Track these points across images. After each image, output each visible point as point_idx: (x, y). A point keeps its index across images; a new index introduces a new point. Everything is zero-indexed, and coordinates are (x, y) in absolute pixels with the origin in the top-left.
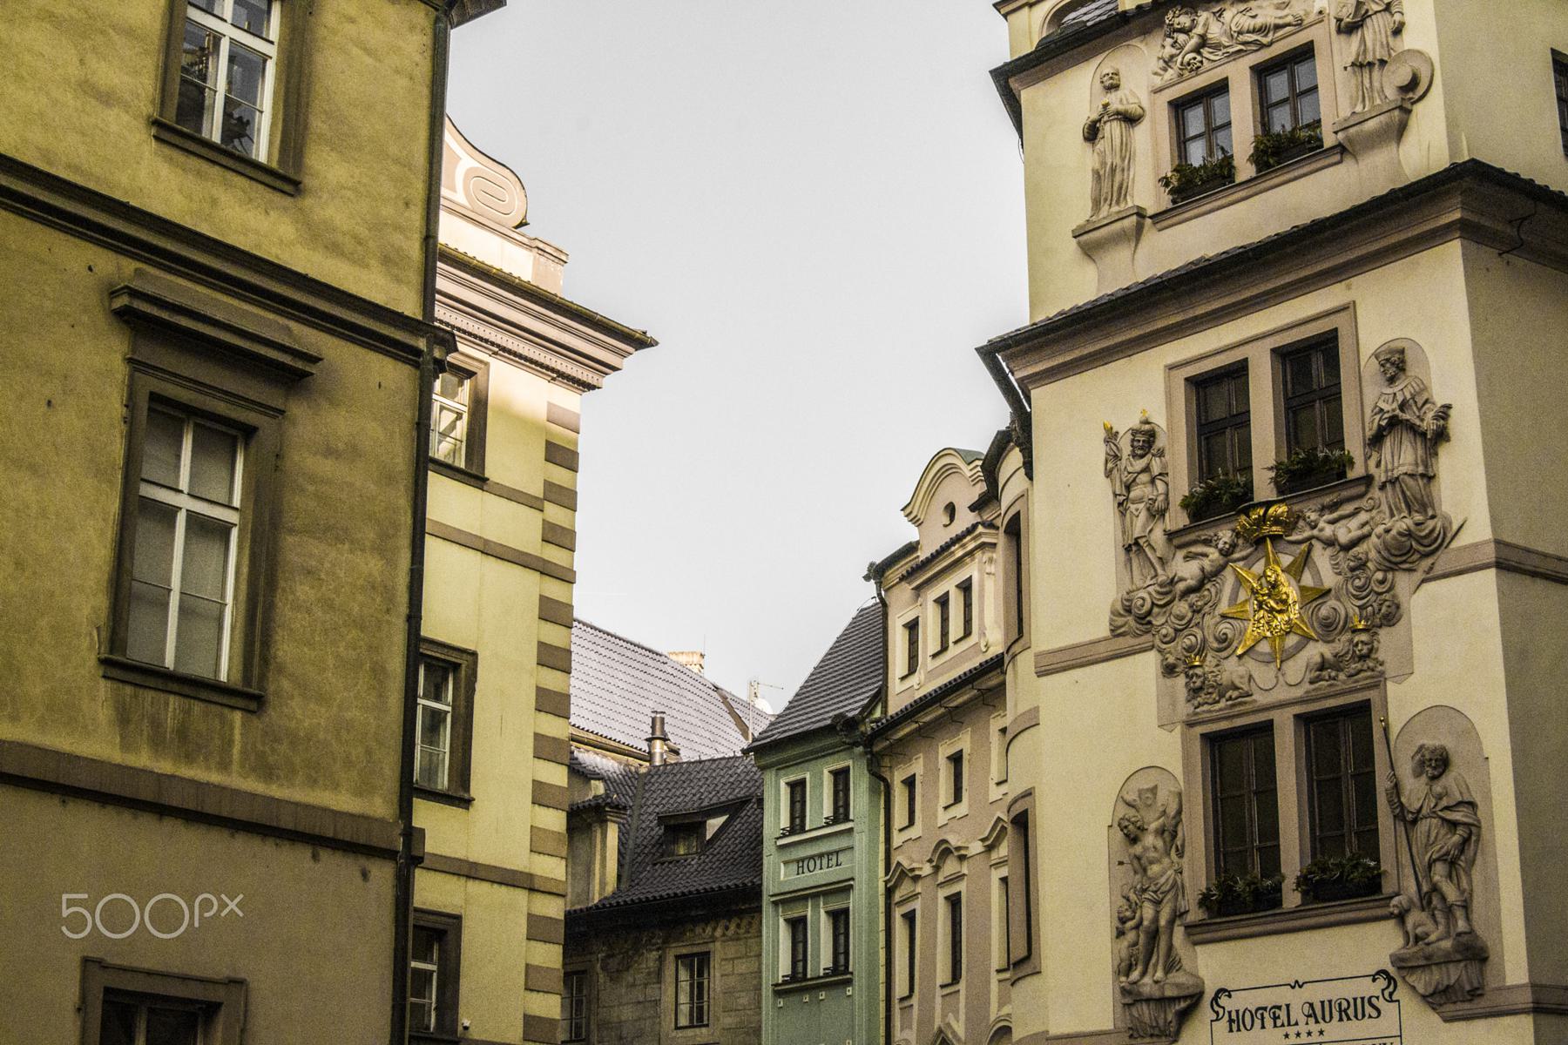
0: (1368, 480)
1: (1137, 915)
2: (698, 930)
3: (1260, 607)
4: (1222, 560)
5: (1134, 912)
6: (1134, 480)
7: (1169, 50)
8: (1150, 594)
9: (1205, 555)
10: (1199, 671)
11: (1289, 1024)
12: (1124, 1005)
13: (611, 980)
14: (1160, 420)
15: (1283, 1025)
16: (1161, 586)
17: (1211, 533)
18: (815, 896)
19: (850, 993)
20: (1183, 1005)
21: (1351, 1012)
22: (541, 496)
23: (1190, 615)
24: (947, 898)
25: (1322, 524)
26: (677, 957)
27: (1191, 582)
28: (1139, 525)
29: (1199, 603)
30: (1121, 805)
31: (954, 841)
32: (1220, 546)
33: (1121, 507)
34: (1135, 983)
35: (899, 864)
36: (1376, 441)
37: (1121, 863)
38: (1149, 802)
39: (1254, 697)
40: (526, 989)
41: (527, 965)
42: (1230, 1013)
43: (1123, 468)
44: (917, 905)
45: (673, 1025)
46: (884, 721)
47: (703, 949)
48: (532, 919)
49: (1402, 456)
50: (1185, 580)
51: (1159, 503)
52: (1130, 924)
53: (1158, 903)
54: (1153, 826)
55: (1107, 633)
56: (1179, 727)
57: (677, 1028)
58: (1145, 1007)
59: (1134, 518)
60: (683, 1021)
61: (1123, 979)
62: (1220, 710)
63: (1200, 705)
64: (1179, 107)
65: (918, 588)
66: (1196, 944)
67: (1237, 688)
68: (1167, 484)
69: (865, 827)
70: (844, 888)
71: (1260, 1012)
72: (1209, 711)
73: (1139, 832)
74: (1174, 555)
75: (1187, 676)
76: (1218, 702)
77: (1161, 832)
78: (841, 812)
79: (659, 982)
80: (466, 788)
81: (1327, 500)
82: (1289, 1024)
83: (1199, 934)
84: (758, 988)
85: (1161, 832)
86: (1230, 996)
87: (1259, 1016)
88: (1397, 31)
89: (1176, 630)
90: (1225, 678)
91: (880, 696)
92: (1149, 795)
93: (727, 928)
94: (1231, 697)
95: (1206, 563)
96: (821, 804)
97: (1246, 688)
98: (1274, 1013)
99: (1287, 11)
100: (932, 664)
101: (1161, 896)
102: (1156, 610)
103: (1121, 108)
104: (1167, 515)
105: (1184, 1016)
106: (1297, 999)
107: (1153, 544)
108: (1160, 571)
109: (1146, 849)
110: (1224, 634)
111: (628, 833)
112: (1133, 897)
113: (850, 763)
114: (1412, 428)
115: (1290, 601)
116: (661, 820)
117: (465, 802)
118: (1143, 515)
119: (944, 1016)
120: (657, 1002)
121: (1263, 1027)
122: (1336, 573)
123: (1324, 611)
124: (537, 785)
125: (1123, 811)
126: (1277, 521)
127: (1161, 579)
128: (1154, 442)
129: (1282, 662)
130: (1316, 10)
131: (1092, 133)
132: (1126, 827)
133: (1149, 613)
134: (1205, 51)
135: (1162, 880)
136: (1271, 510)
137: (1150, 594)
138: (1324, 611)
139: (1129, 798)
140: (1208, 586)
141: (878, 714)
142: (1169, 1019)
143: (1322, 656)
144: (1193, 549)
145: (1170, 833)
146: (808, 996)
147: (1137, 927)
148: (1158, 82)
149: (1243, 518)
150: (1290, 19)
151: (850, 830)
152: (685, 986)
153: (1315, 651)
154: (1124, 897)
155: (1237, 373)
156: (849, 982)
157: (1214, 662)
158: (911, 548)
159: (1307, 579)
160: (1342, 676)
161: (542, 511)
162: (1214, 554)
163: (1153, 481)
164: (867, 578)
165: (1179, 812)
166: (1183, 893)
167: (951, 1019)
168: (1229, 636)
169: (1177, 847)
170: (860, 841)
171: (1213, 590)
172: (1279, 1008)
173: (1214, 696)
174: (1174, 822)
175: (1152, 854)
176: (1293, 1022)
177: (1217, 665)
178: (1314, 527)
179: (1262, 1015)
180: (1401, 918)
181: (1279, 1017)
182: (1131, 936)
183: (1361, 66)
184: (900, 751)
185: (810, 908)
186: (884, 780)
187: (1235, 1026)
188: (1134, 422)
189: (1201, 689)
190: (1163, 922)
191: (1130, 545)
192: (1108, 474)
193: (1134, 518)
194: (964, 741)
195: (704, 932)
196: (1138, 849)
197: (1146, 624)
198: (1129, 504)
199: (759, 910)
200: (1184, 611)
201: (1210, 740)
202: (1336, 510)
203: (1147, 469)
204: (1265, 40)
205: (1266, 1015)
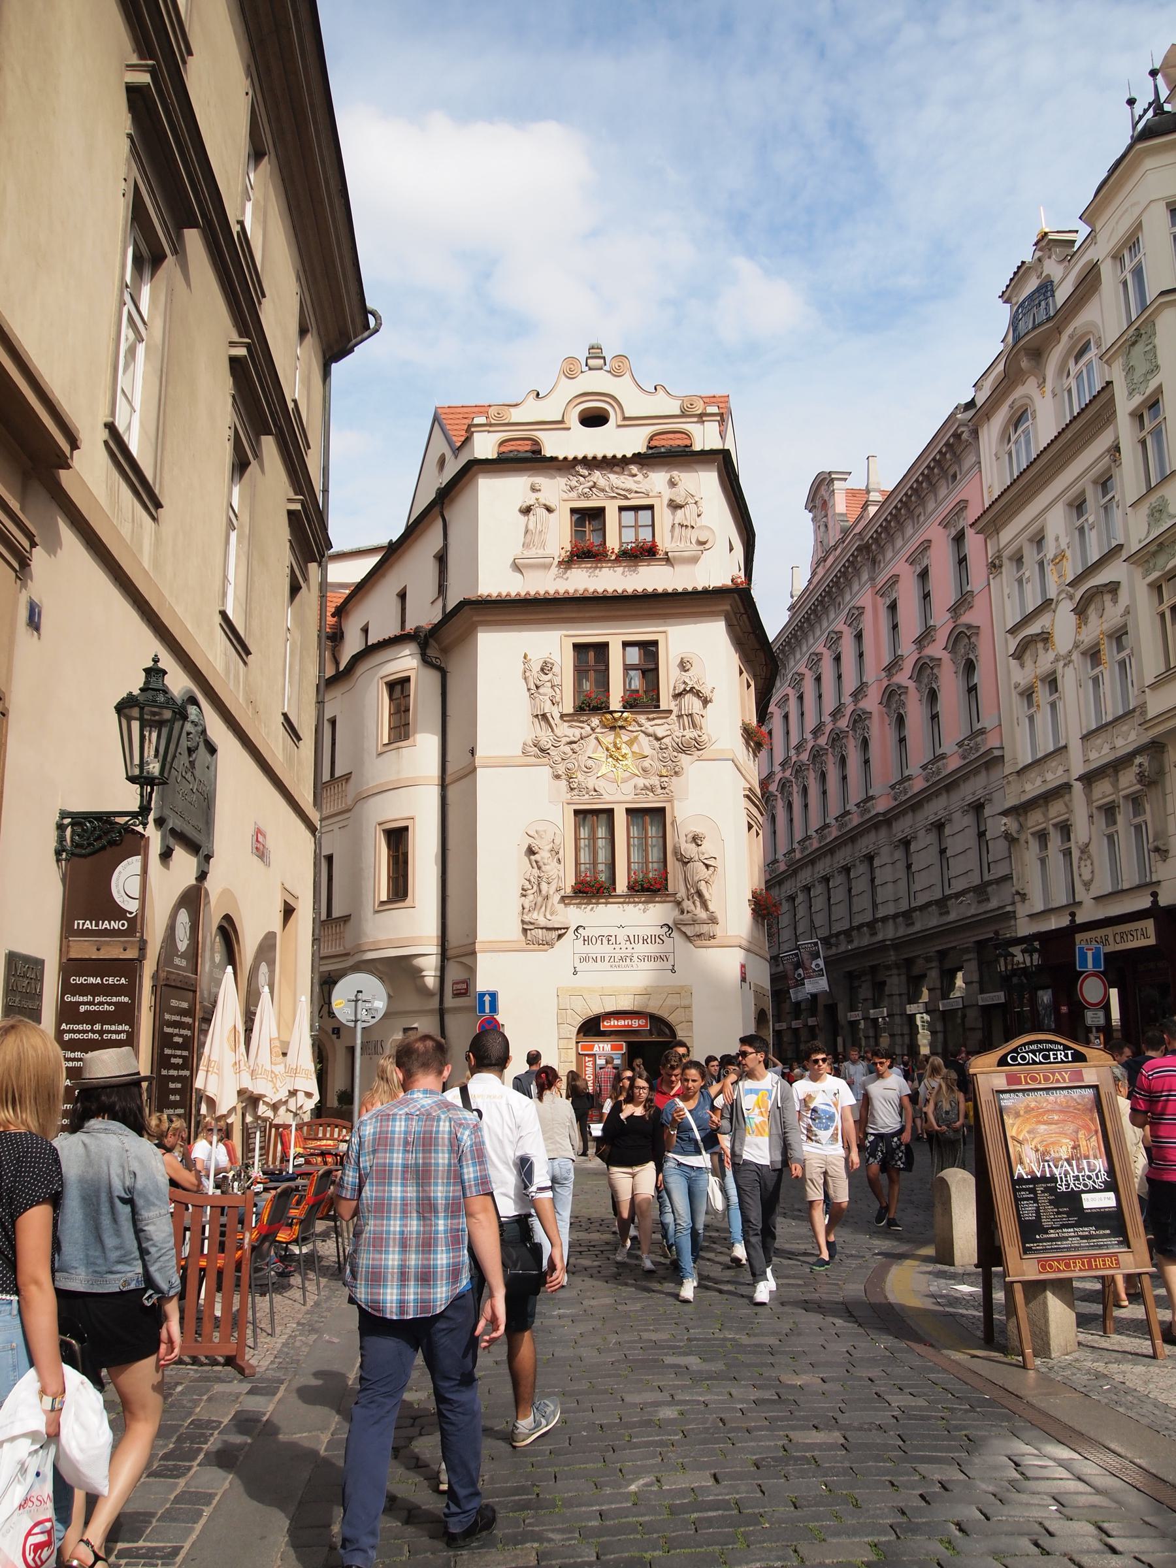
0: (670, 712)
3: (611, 756)
7: (574, 483)
9: (582, 728)
14: (556, 658)
17: (585, 718)
20: (563, 931)
21: (649, 941)
27: (573, 739)
28: (548, 708)
36: (678, 696)
49: (692, 703)
51: (558, 699)
52: (529, 892)
64: (573, 511)
67: (595, 791)
81: (651, 716)
88: (699, 516)
90: (591, 787)
95: (582, 731)
99: (640, 486)
103: (548, 503)
105: (560, 936)
106: (621, 935)
109: (542, 858)
114: (698, 694)
126: (626, 720)
130: (657, 489)
131: (526, 511)
134: (593, 489)
135: (551, 874)
136: (625, 715)
138: (646, 763)
148: (565, 496)
149: (609, 716)
150: (643, 490)
153: (641, 782)
155: (602, 649)
159: (635, 748)
160: (651, 794)
162: (588, 728)
175: (546, 861)
180: (679, 903)
182: (531, 897)
183: (682, 526)
190: (551, 893)
196: (537, 857)
204: (629, 496)
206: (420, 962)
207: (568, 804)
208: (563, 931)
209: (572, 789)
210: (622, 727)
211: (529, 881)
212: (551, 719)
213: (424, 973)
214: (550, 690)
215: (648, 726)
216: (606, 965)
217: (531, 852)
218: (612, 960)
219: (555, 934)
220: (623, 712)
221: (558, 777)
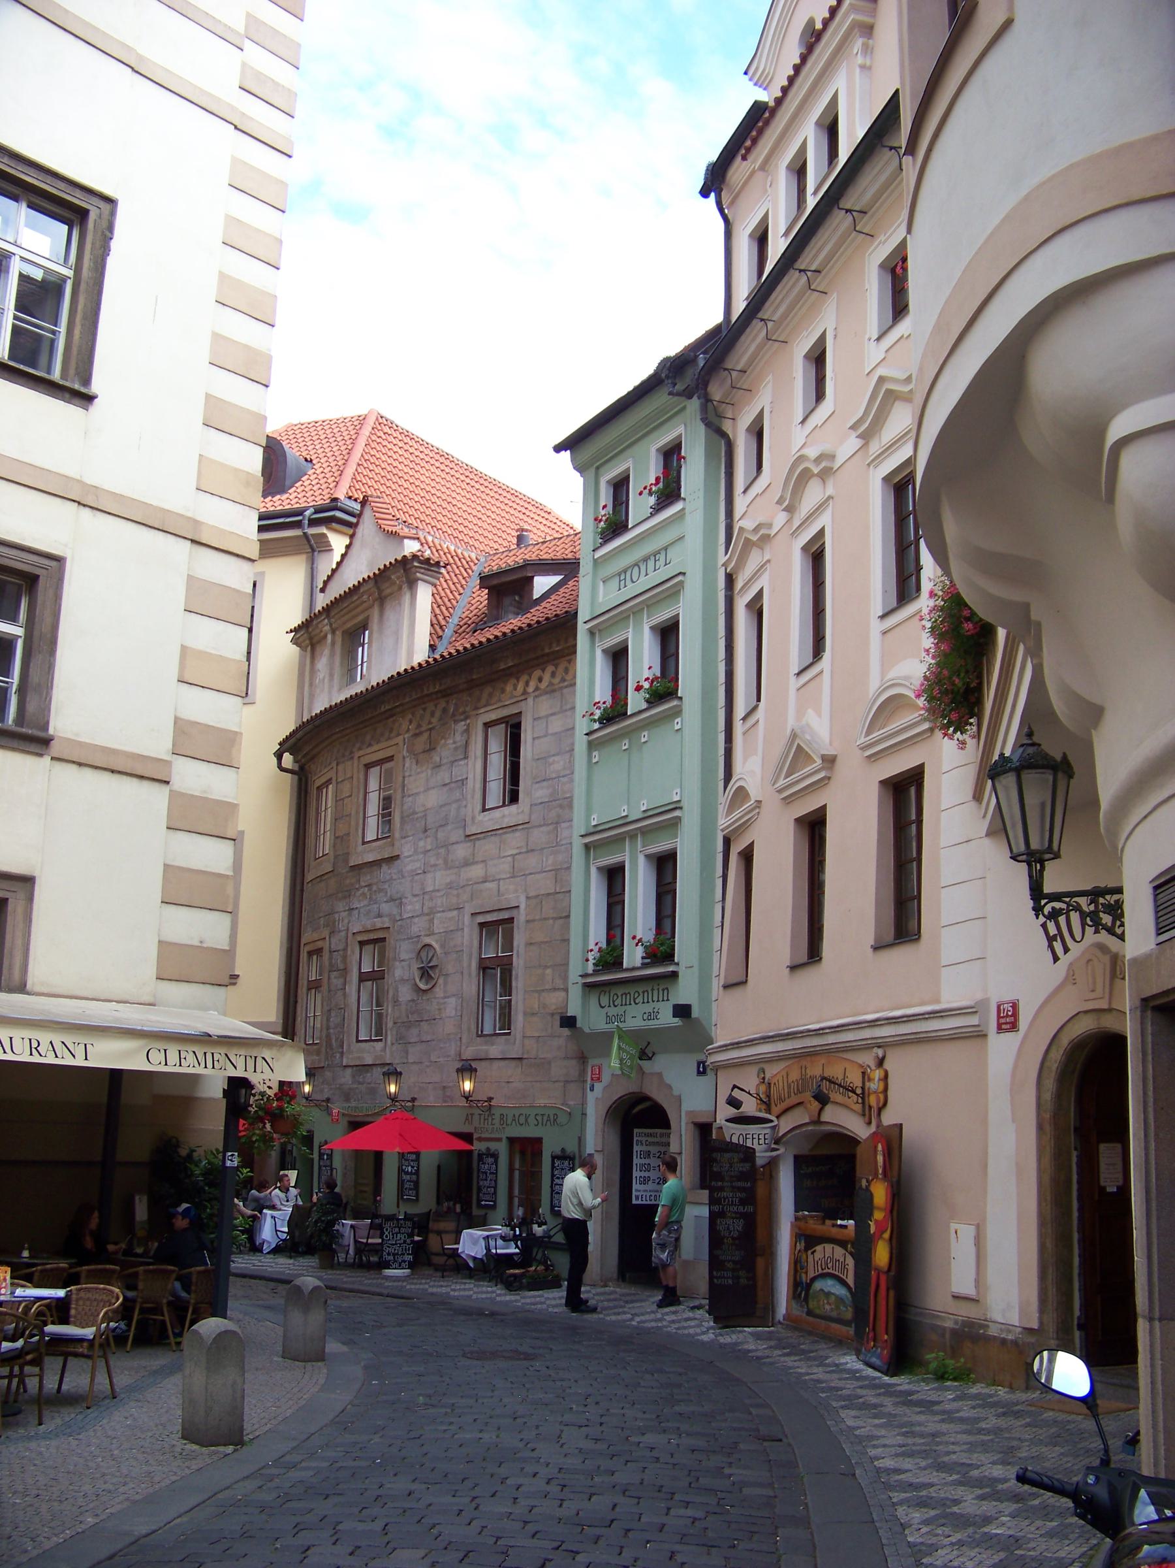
2: (509, 688)
13: (417, 762)
18: (636, 612)
26: (487, 725)
35: (741, 529)
41: (184, 649)
45: (479, 807)
47: (514, 710)
48: (193, 583)
57: (484, 810)
60: (494, 799)
69: (700, 503)
70: (671, 589)
79: (466, 758)
80: (87, 380)
93: (540, 680)
111: (454, 608)
113: (680, 430)
116: (486, 580)
117: (86, 399)
119: (800, 712)
120: (463, 782)
146: (627, 741)
151: (681, 514)
156: (677, 712)
164: (704, 193)
167: (811, 717)
184: (743, 390)
186: (723, 434)
195: (515, 689)
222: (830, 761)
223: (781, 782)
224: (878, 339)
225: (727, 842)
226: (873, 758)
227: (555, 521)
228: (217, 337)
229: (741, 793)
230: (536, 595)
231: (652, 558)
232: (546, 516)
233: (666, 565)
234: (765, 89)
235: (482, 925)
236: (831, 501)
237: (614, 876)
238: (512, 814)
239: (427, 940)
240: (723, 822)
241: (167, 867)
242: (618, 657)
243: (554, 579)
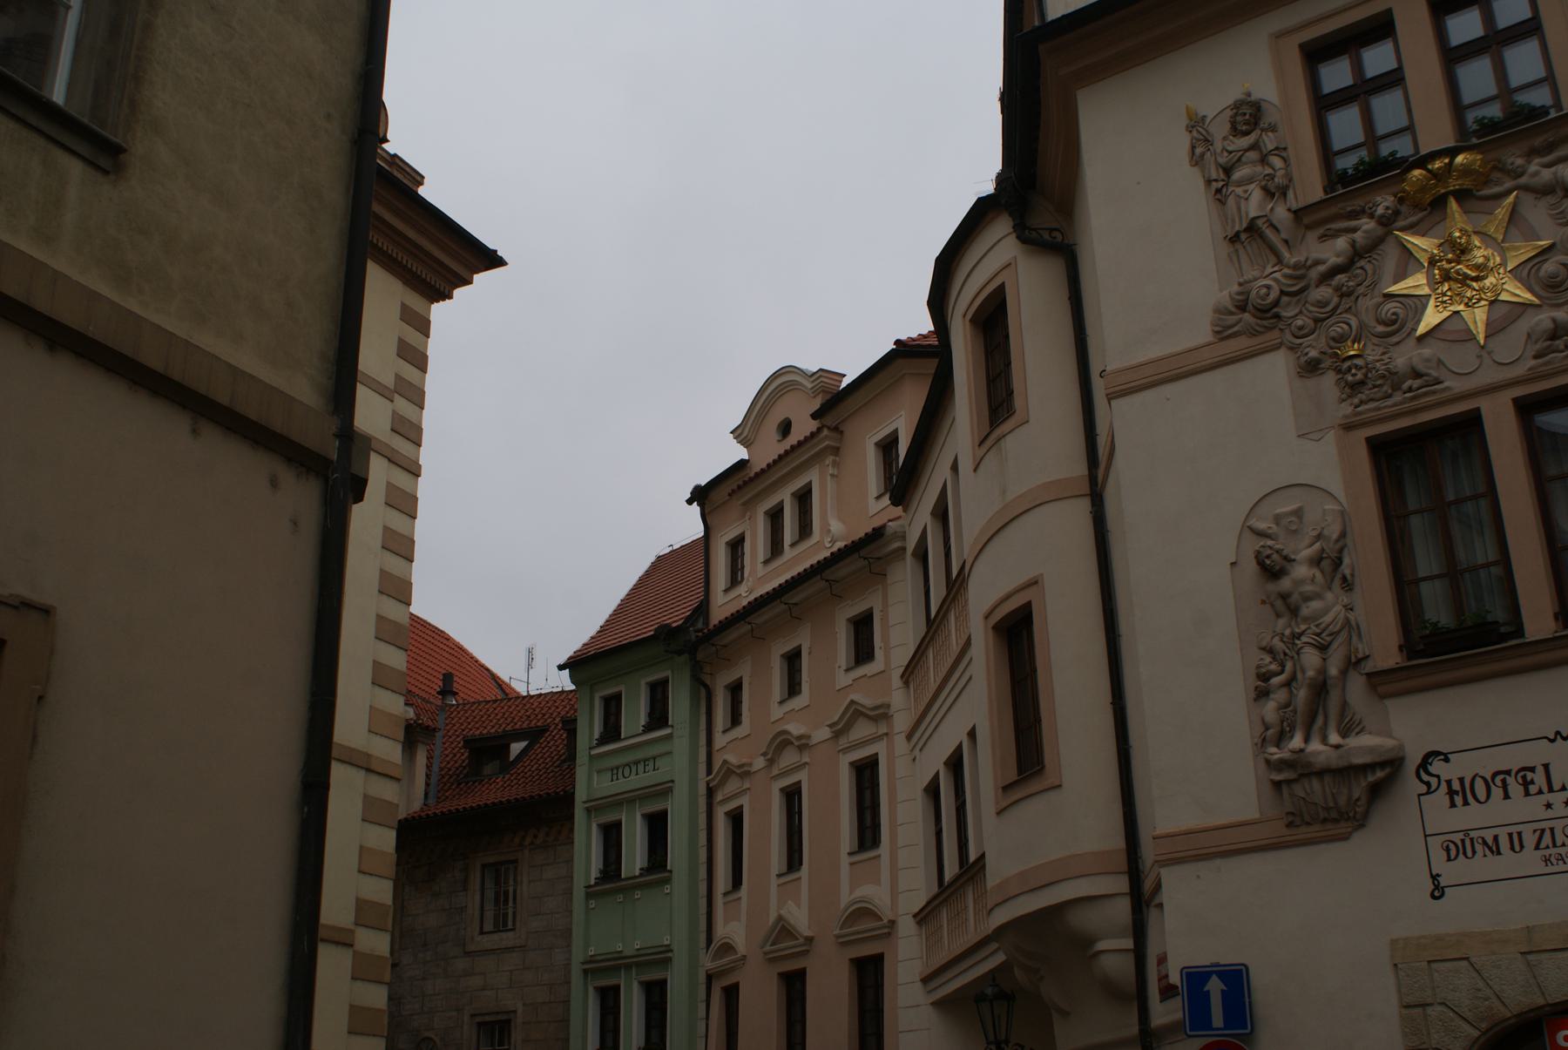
1: (1289, 666)
3: (1446, 277)
4: (1380, 231)
5: (1283, 666)
6: (1239, 159)
8: (1276, 280)
9: (1355, 230)
10: (1358, 362)
11: (1551, 790)
12: (1277, 785)
14: (1265, 88)
15: (1540, 792)
16: (1296, 267)
17: (1357, 203)
18: (631, 801)
19: (668, 891)
20: (1380, 774)
22: (392, 388)
23: (1336, 300)
24: (782, 790)
25: (1533, 168)
27: (1334, 260)
28: (1255, 204)
29: (1351, 284)
30: (1248, 534)
31: (795, 729)
32: (1380, 211)
33: (1220, 196)
34: (1302, 751)
35: (725, 762)
37: (1263, 602)
38: (1294, 528)
39: (1446, 384)
40: (360, 871)
42: (1449, 782)
43: (1219, 150)
44: (744, 801)
46: (706, 631)
50: (1323, 262)
51: (1279, 179)
52: (1276, 680)
53: (1323, 648)
54: (1306, 553)
55: (1210, 338)
56: (1331, 436)
57: (482, 933)
58: (1316, 784)
59: (1243, 203)
60: (488, 927)
61: (1273, 750)
62: (1395, 405)
63: (1362, 402)
65: (744, 504)
66: (1383, 697)
67: (1417, 375)
68: (1283, 158)
70: (665, 790)
71: (1502, 776)
72: (1378, 409)
73: (1285, 563)
74: (1304, 236)
75: (1339, 371)
76: (1390, 396)
77: (1316, 561)
78: (658, 718)
79: (465, 889)
81: (1538, 141)
82: (1551, 790)
83: (1383, 683)
84: (569, 893)
85: (1316, 561)
86: (1447, 760)
87: (1499, 784)
89: (1317, 321)
91: (703, 609)
92: (1293, 519)
93: (535, 837)
94: (1410, 390)
95: (1358, 236)
96: (635, 714)
97: (1434, 373)
98: (1524, 777)
100: (761, 570)
101: (1328, 639)
102: (1285, 299)
104: (1290, 195)
105: (1377, 791)
107: (1275, 222)
108: (1286, 254)
109: (1299, 583)
110: (1394, 314)
112: (1277, 644)
113: (668, 673)
115: (1491, 264)
116: (469, 743)
118: (1257, 195)
121: (1507, 796)
122: (1560, 224)
123: (1550, 267)
124: (377, 665)
125: (1255, 544)
126: (1466, 171)
127: (1293, 260)
128: (1260, 119)
129: (1486, 337)
132: (1268, 557)
133: (1276, 303)
135: (1327, 619)
136: (1460, 159)
137: (1276, 280)
138: (1550, 267)
139: (1261, 526)
140: (1358, 265)
141: (700, 625)
142: (1356, 794)
143: (1554, 320)
144: (1334, 226)
145: (1331, 562)
146: (621, 896)
147: (1288, 684)
149: (1417, 172)
151: (669, 737)
152: (490, 894)
153: (1544, 319)
154: (1263, 649)
156: (668, 881)
157: (1381, 350)
158: (741, 465)
161: (392, 401)
163: (1263, 160)
164: (690, 502)
165: (1343, 535)
166: (1360, 635)
168: (1401, 316)
169: (1344, 579)
170: (681, 745)
171: (1369, 267)
172: (1532, 769)
173: (1385, 388)
174: (1338, 546)
175: (1308, 588)
176: (1556, 786)
177: (1384, 354)
178: (1521, 175)
179: (1504, 781)
181: (1532, 782)
185: (624, 814)
187: (1458, 800)
188: (1234, 94)
189: (1362, 383)
190: (1333, 671)
191: (1237, 235)
192: (1197, 160)
193: (1242, 200)
194: (803, 638)
196: (1285, 584)
197: (1271, 318)
198: (1230, 189)
199: (571, 818)
200: (1326, 295)
201: (1378, 447)
202: (1549, 153)
203: (1254, 147)
205: (1510, 780)
206: (1087, 920)
207: (1348, 427)
208: (1380, 774)
209: (1355, 387)
210: (1462, 196)
211: (1270, 651)
212: (1269, 233)
213: (1102, 945)
214: (1259, 169)
215: (1539, 172)
216: (1530, 860)
217: (1271, 569)
218: (1547, 839)
219: (1359, 789)
220: (1452, 152)
221: (1311, 368)
222: (810, 940)
223: (768, 948)
224: (847, 670)
225: (710, 978)
226: (844, 944)
227: (453, 647)
228: (380, 618)
229: (727, 948)
230: (511, 759)
231: (642, 763)
232: (445, 642)
233: (654, 770)
234: (746, 447)
235: (480, 1024)
236: (807, 766)
237: (609, 1001)
238: (507, 939)
239: (427, 1034)
240: (707, 963)
241: (352, 1006)
242: (612, 834)
243: (523, 744)
